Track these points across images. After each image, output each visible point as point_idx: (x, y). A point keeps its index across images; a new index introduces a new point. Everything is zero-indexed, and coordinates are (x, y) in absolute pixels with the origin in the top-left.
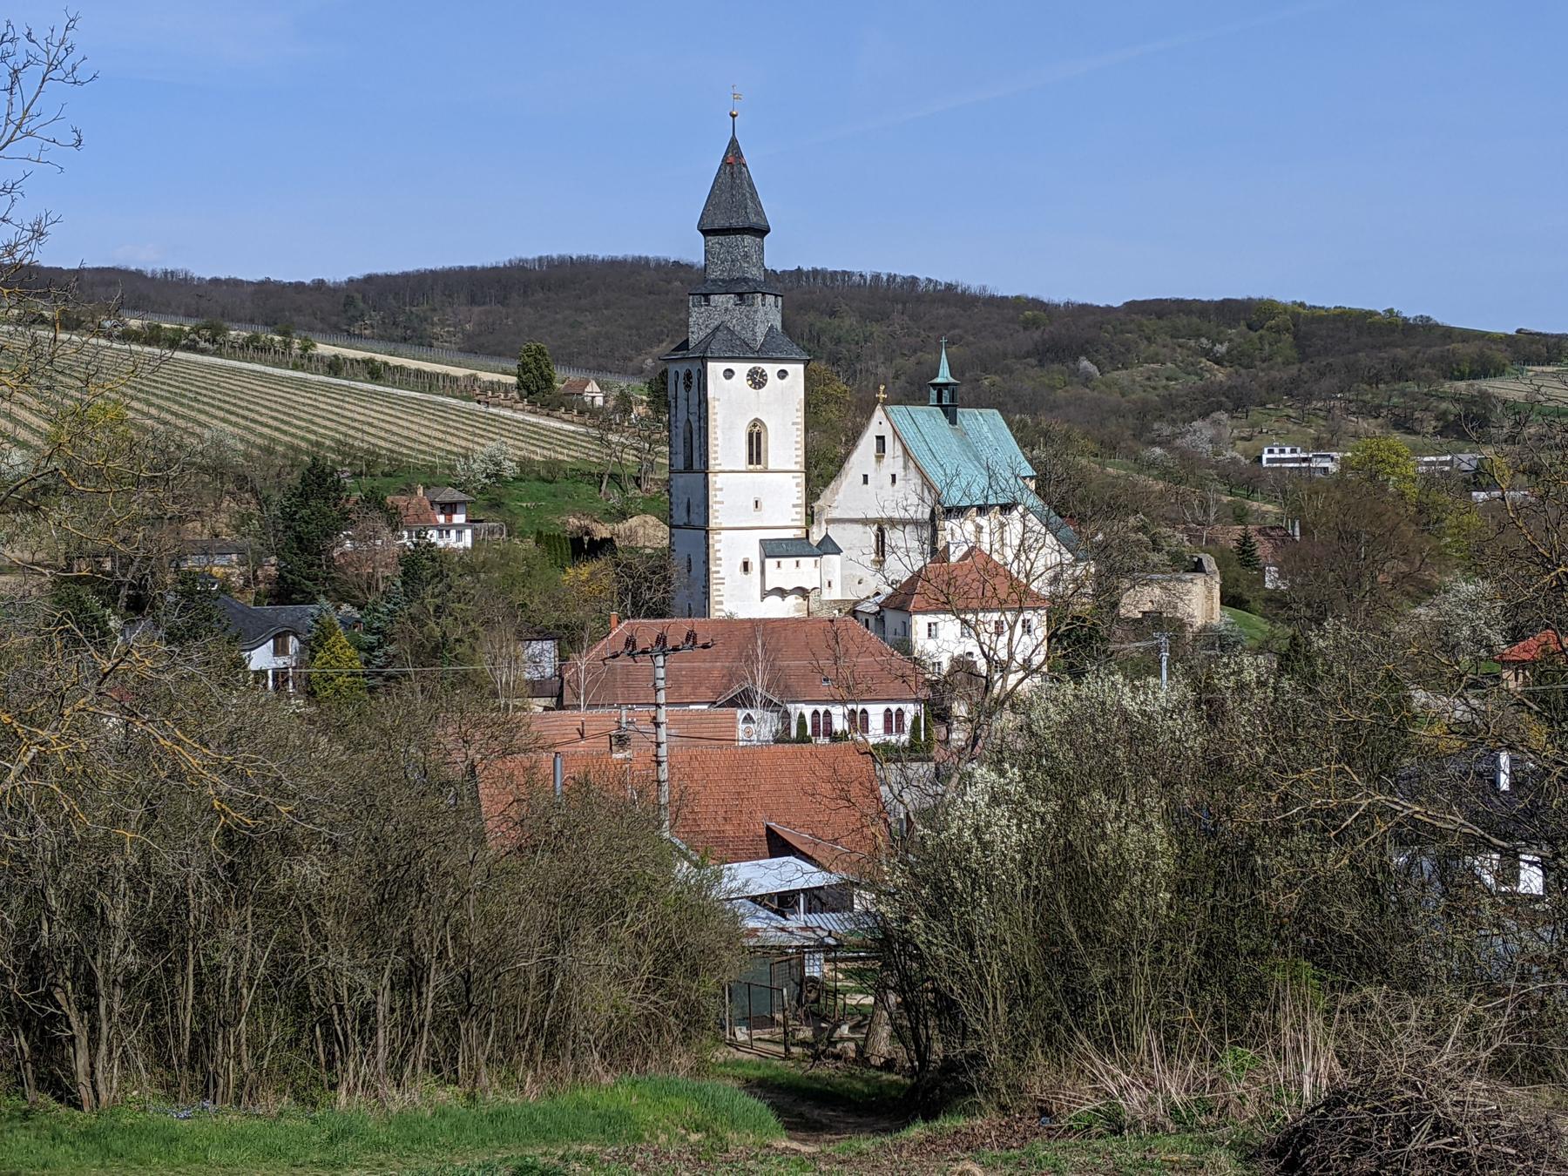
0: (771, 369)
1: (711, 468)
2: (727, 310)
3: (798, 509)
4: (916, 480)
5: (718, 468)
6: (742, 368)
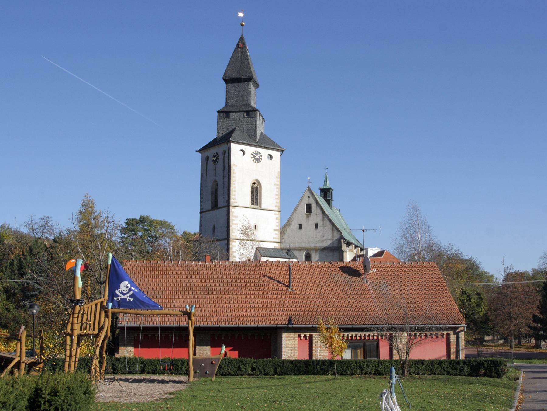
0: (264, 152)
1: (231, 204)
2: (240, 120)
3: (277, 232)
4: (329, 226)
5: (235, 204)
6: (250, 150)
